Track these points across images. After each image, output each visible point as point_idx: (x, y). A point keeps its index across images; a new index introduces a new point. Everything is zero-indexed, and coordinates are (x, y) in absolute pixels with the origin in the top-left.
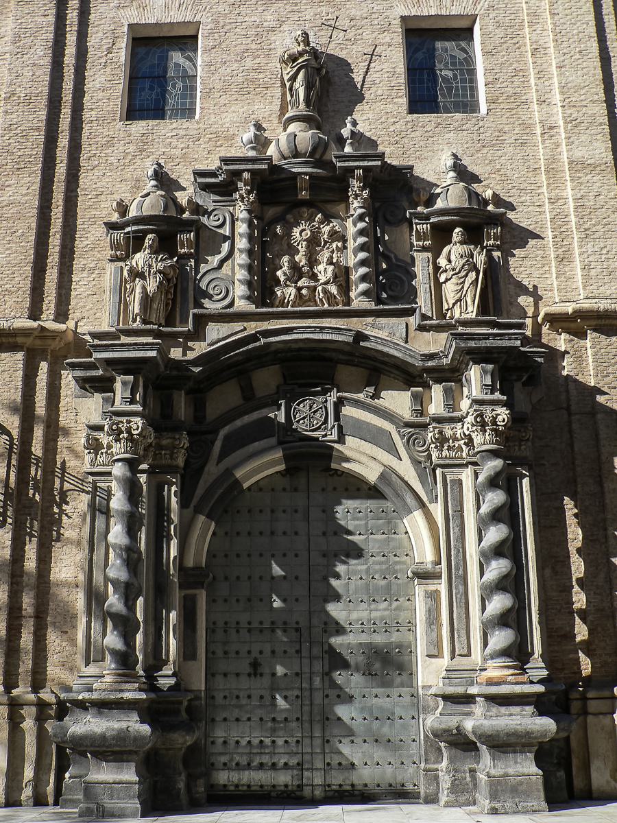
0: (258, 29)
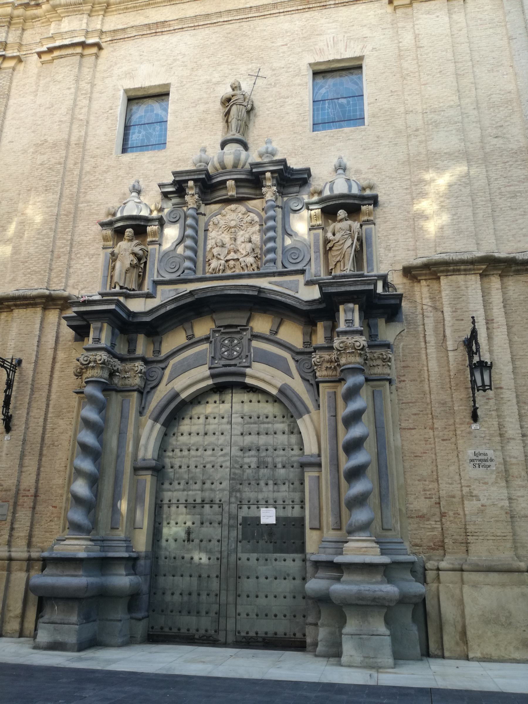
0: (209, 84)
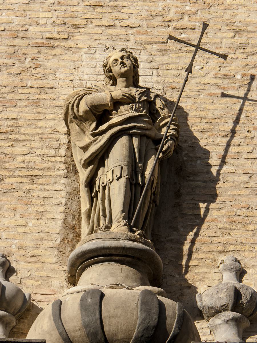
0: (17, 42)
